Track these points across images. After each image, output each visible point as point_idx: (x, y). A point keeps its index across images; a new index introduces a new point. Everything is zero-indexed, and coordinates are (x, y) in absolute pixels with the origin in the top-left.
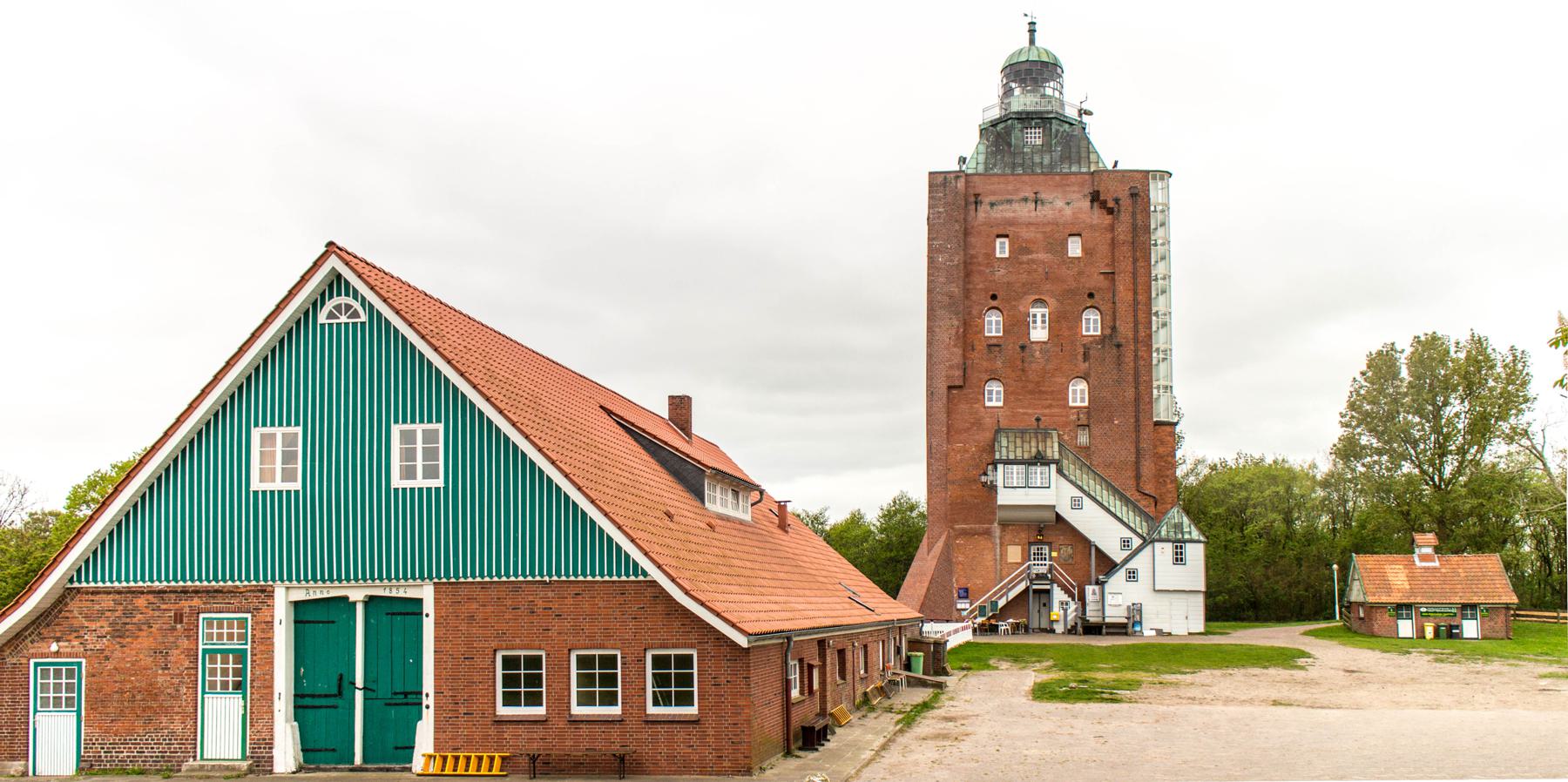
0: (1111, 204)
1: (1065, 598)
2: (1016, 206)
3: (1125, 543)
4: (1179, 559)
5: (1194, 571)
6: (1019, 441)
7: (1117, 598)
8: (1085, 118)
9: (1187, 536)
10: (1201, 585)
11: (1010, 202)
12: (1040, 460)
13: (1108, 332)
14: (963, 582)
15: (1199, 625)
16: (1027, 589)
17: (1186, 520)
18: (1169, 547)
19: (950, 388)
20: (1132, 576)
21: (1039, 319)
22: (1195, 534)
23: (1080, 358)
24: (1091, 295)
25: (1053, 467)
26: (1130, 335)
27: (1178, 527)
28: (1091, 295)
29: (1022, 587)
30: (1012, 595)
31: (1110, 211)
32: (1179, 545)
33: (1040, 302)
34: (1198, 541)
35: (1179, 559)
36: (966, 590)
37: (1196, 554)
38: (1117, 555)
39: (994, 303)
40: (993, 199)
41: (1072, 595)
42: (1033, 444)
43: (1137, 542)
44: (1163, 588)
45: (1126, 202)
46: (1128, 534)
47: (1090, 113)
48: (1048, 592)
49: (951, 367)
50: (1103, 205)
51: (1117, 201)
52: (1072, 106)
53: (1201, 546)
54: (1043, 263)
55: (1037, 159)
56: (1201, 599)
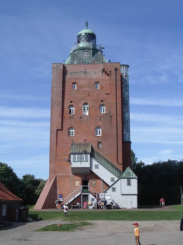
0: (108, 73)
1: (93, 197)
2: (79, 74)
3: (112, 179)
4: (129, 184)
5: (134, 187)
6: (79, 147)
7: (109, 197)
8: (102, 50)
9: (131, 177)
10: (137, 193)
11: (77, 72)
12: (86, 153)
13: (108, 112)
14: (61, 193)
15: (135, 205)
16: (80, 195)
17: (131, 171)
18: (126, 180)
19: (57, 130)
20: (114, 190)
21: (86, 108)
22: (134, 176)
23: (99, 120)
24: (102, 101)
25: (89, 155)
26: (115, 113)
27: (129, 173)
28: (102, 101)
29: (79, 194)
30: (76, 196)
31: (108, 75)
32: (129, 179)
33: (86, 104)
34: (136, 178)
35: (129, 184)
36: (62, 195)
37: (134, 182)
38: (110, 184)
39: (71, 104)
40: (71, 72)
41: (95, 196)
42: (83, 148)
43: (116, 179)
44: (124, 193)
45: (113, 72)
46: (113, 176)
47: (103, 48)
48: (88, 195)
49: (58, 124)
50: (106, 73)
51: (110, 72)
52: (98, 46)
53: (136, 180)
54: (87, 91)
55: (87, 61)
56: (136, 197)
